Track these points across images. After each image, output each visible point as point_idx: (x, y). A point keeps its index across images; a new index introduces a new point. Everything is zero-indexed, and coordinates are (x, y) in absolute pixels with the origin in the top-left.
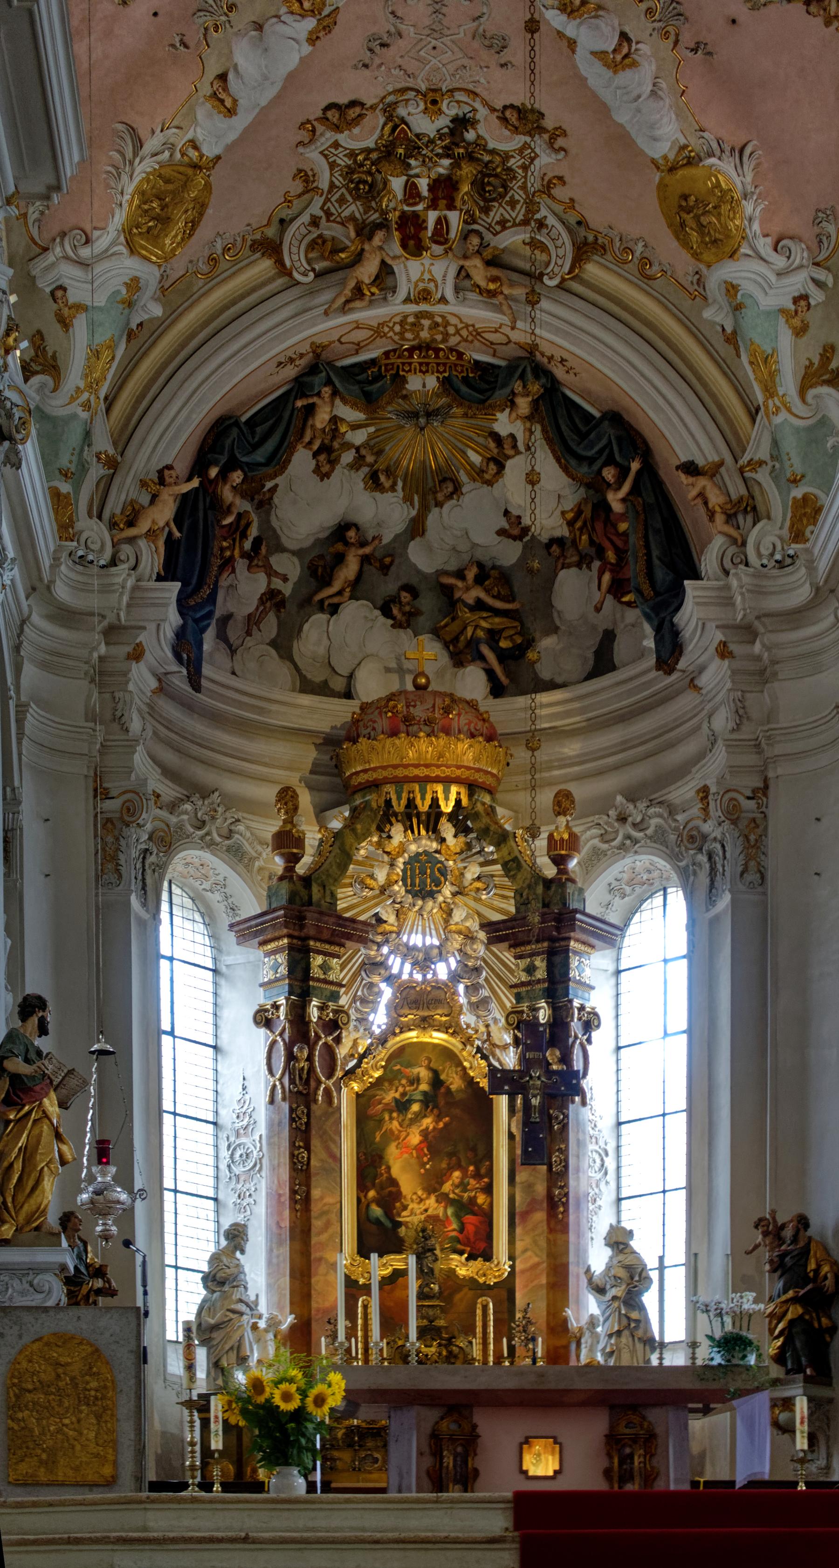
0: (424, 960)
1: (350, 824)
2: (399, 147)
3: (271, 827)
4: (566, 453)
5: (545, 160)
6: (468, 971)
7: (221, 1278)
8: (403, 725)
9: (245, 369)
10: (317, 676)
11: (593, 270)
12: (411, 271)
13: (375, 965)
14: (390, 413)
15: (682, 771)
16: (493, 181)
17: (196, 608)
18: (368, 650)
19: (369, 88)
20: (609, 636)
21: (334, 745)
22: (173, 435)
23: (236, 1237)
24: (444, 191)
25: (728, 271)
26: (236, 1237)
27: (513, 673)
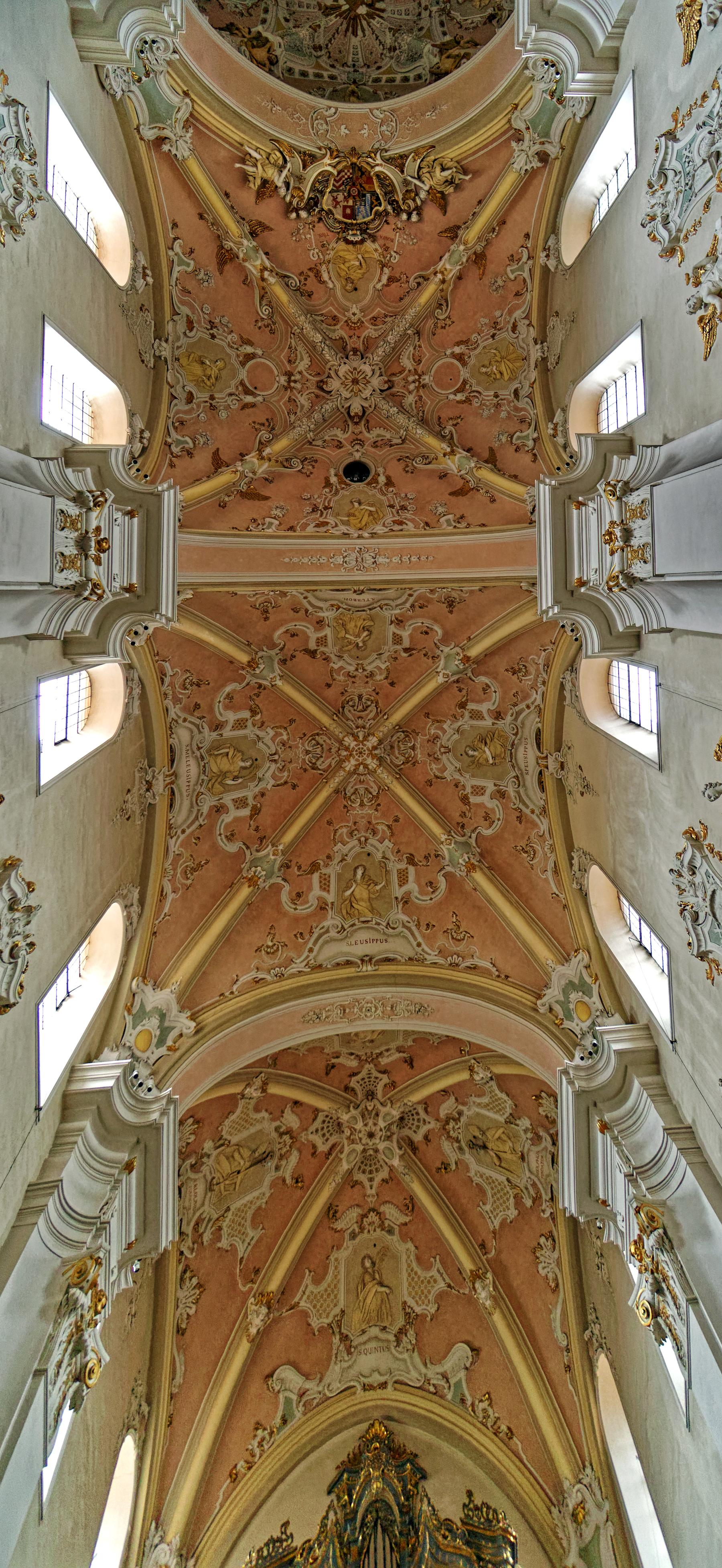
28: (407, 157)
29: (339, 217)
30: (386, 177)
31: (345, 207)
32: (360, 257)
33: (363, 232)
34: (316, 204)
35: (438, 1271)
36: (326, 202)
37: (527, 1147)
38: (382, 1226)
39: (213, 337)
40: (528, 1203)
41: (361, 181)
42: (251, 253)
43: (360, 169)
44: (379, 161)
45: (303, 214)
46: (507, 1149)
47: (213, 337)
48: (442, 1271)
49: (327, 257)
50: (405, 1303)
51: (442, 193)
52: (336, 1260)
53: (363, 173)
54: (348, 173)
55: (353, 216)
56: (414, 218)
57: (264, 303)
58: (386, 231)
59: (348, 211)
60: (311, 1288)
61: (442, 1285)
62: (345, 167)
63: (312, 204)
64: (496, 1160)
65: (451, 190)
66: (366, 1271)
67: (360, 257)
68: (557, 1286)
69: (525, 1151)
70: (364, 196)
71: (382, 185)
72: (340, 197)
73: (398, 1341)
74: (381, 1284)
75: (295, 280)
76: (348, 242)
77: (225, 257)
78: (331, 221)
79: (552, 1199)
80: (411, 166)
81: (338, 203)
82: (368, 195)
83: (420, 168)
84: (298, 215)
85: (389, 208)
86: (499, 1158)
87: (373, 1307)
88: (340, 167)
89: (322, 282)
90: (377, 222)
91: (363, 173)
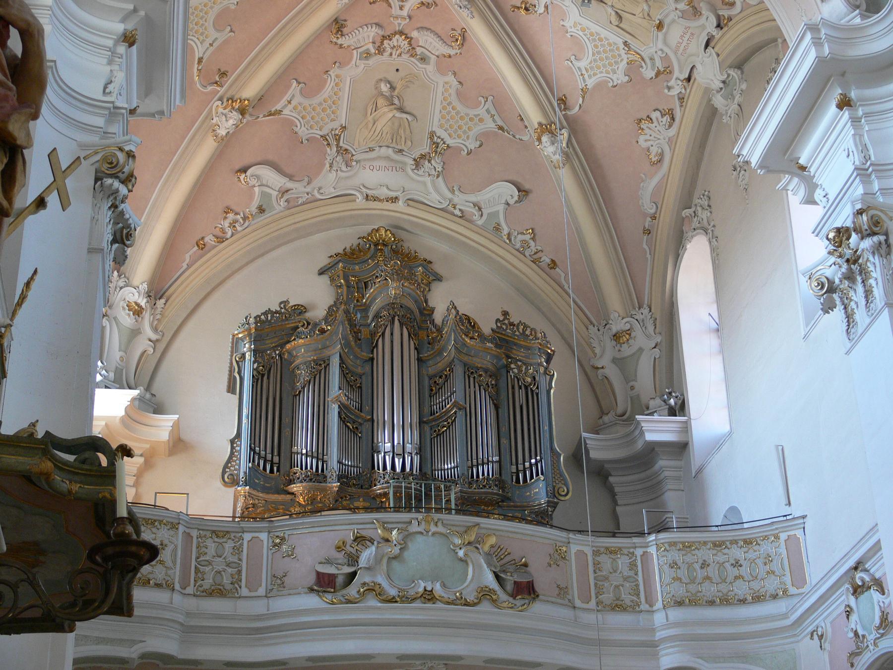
35: (488, 111)
37: (672, 16)
38: (412, 53)
40: (649, 73)
46: (637, 11)
48: (493, 112)
50: (432, 134)
52: (337, 76)
60: (298, 99)
61: (490, 125)
64: (614, 18)
66: (382, 94)
68: (660, 161)
69: (667, 22)
73: (417, 164)
74: (401, 110)
79: (689, 79)
86: (620, 17)
87: (386, 130)
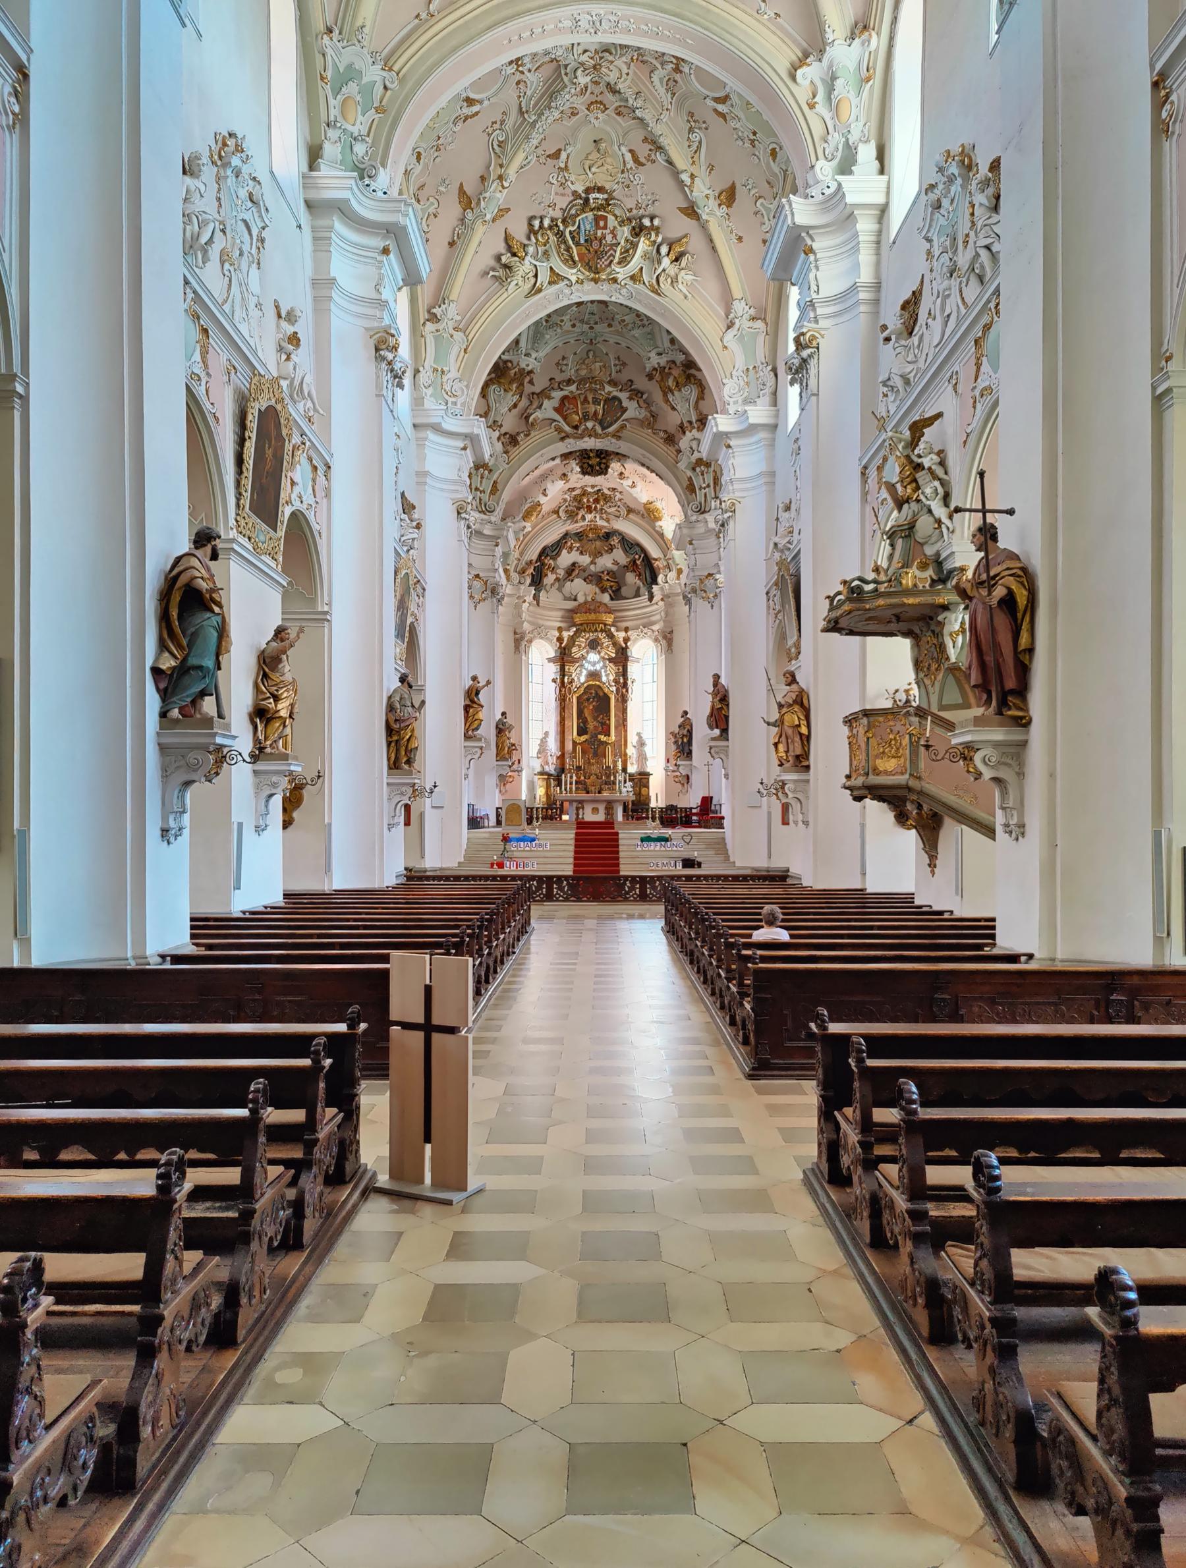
0: (594, 664)
1: (576, 633)
2: (584, 493)
3: (557, 635)
4: (625, 551)
5: (618, 496)
6: (605, 666)
7: (543, 742)
8: (588, 611)
9: (551, 536)
10: (568, 595)
11: (631, 516)
12: (589, 517)
13: (582, 666)
14: (585, 541)
15: (653, 623)
16: (607, 499)
17: (538, 590)
18: (581, 589)
19: (578, 485)
20: (639, 588)
21: (573, 611)
22: (533, 554)
23: (546, 734)
24: (596, 501)
25: (659, 523)
26: (546, 734)
27: (616, 595)
28: (550, 283)
29: (611, 218)
30: (565, 262)
31: (605, 227)
32: (590, 175)
33: (587, 200)
34: (634, 228)
36: (625, 232)
39: (755, 133)
41: (590, 256)
42: (701, 203)
43: (590, 269)
44: (574, 279)
45: (646, 222)
47: (755, 133)
49: (625, 175)
51: (514, 255)
53: (588, 264)
54: (603, 263)
55: (597, 219)
56: (536, 223)
57: (694, 147)
58: (562, 203)
59: (602, 224)
62: (604, 270)
63: (638, 231)
65: (504, 259)
67: (590, 175)
70: (586, 241)
71: (568, 249)
72: (609, 238)
75: (660, 158)
76: (600, 190)
77: (729, 196)
78: (618, 213)
80: (544, 277)
81: (612, 232)
82: (582, 241)
83: (536, 276)
84: (652, 221)
85: (562, 228)
88: (609, 270)
89: (631, 151)
90: (573, 212)
91: (588, 264)
